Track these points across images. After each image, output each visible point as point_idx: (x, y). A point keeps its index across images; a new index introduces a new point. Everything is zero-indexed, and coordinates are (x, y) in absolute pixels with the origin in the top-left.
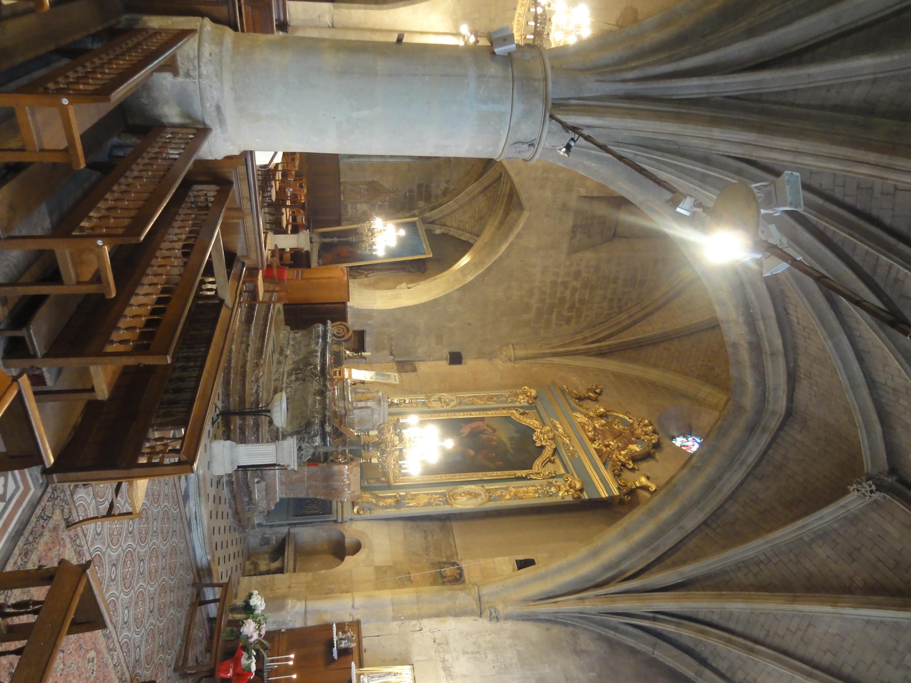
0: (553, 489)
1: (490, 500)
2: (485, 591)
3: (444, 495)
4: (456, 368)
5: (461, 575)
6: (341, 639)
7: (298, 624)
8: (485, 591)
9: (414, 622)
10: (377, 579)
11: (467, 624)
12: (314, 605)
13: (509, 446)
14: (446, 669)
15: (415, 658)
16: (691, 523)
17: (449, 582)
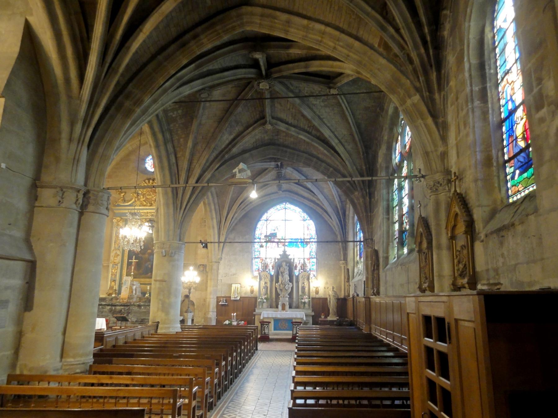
2: (214, 260)
5: (203, 265)
7: (215, 314)
8: (214, 260)
11: (221, 266)
12: (211, 309)
14: (234, 275)
15: (229, 282)
16: (216, 201)
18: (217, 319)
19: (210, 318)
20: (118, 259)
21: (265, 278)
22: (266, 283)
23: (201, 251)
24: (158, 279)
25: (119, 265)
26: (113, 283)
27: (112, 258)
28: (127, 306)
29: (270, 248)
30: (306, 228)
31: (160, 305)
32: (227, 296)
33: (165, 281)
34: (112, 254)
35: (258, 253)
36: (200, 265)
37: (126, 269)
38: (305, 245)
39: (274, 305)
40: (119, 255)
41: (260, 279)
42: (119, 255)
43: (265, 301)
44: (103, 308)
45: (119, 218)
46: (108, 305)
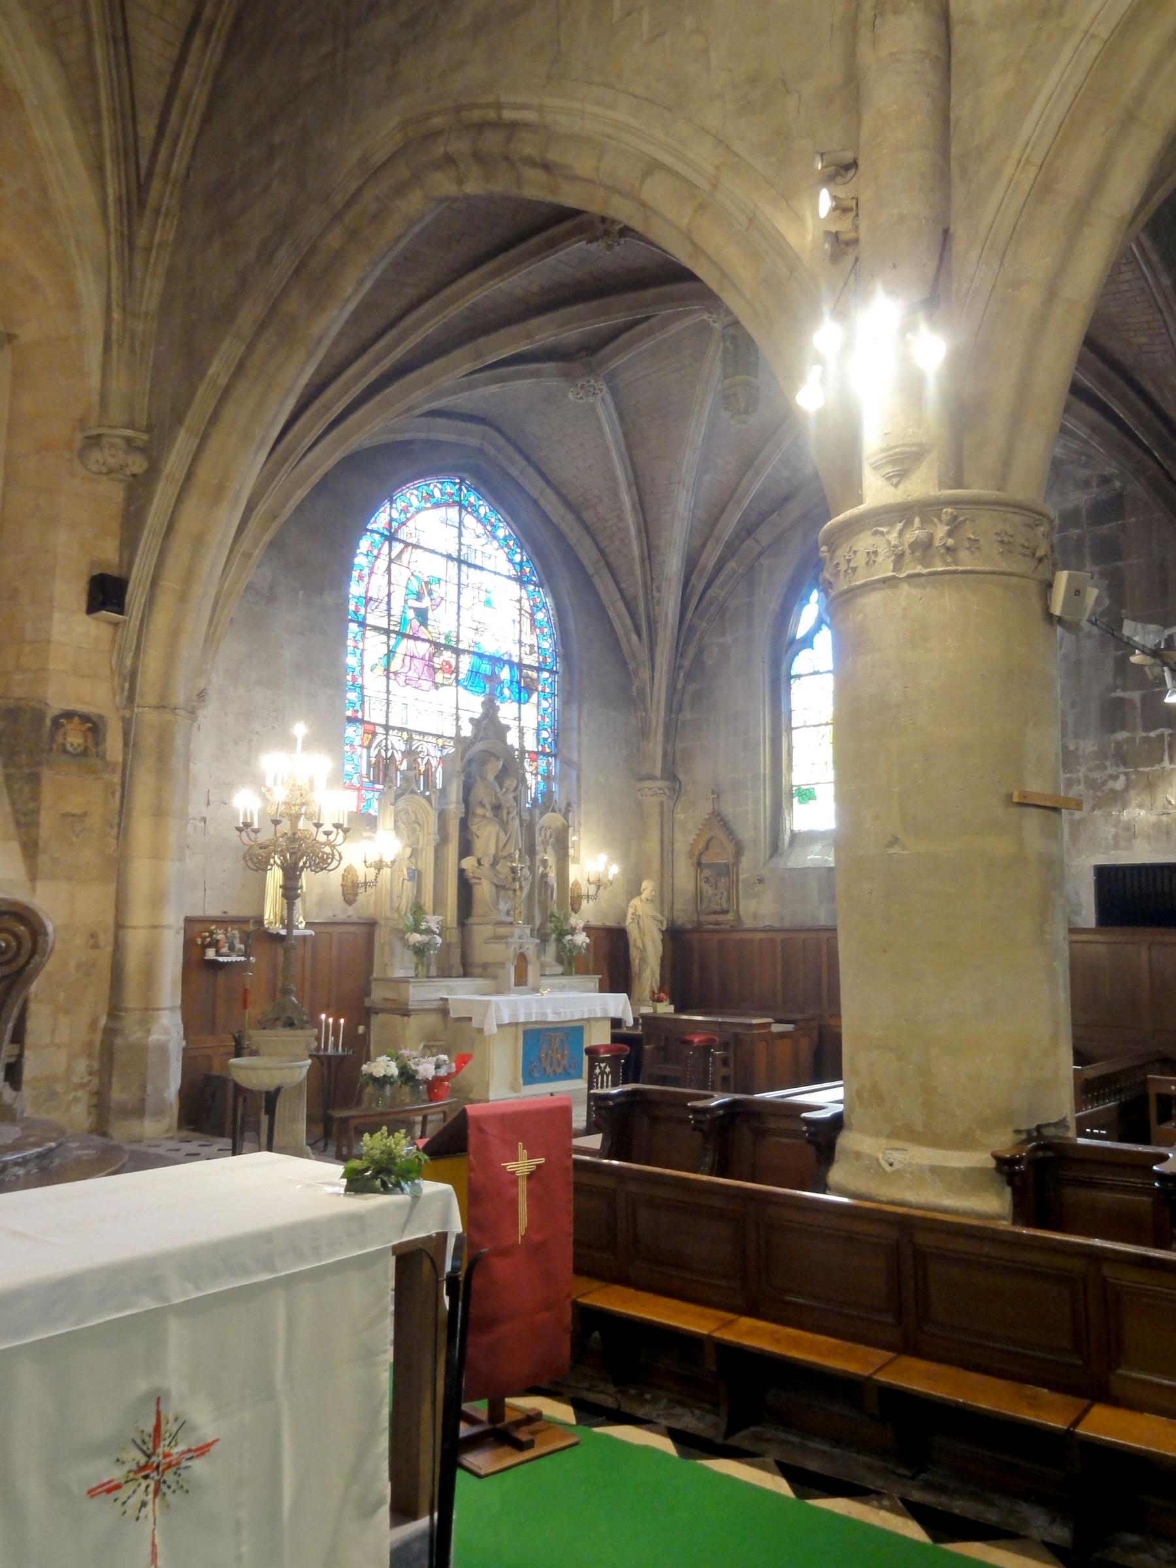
5: (85, 718)
6: (232, 948)
9: (190, 828)
10: (69, 879)
17: (97, 744)
18: (184, 1050)
19: (163, 1049)
23: (74, 630)
29: (402, 678)
30: (526, 623)
32: (233, 912)
36: (69, 715)
38: (524, 695)
39: (456, 959)
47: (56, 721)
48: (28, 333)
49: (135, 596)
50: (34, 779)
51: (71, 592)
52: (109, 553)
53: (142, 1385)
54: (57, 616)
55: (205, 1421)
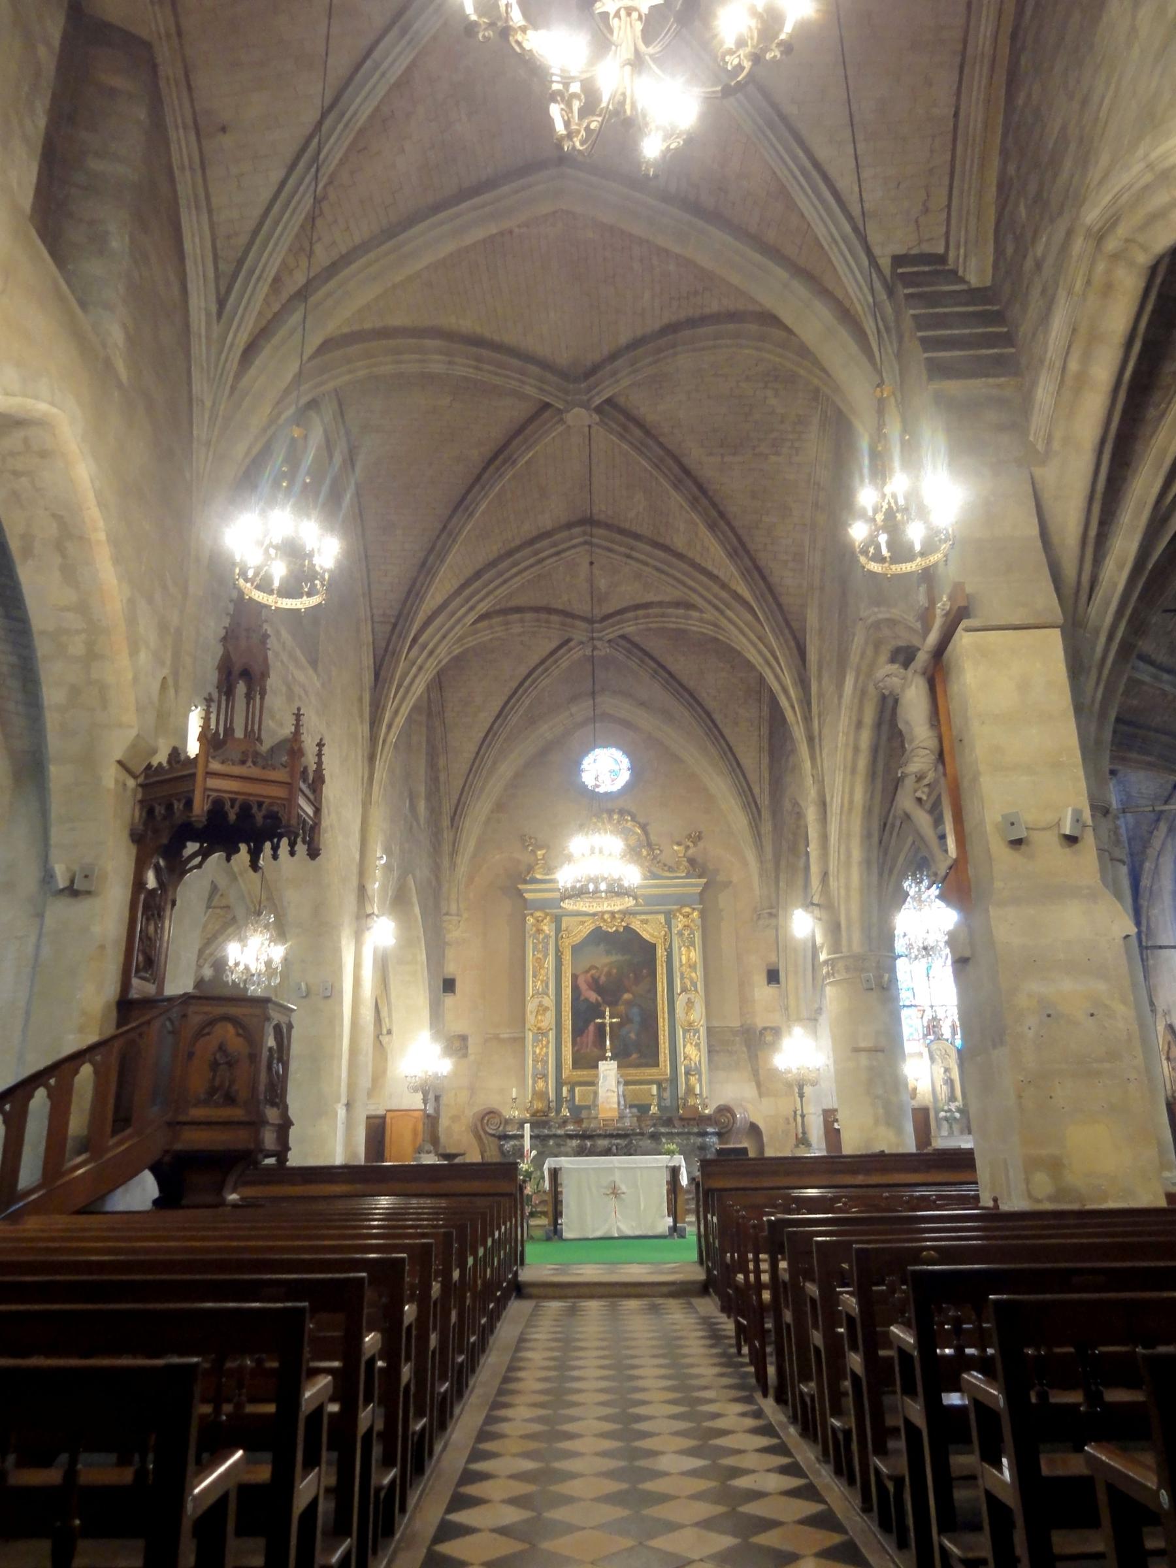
0: (686, 933)
1: (696, 990)
3: (685, 1031)
4: (458, 985)
5: (772, 1029)
13: (614, 958)
20: (548, 1020)
21: (943, 1059)
22: (947, 1070)
23: (763, 992)
24: (863, 1045)
25: (552, 1035)
26: (541, 1084)
27: (531, 1019)
28: (625, 1136)
31: (881, 1111)
33: (882, 1051)
34: (531, 1006)
35: (910, 994)
36: (765, 1029)
37: (570, 1045)
40: (547, 1009)
41: (932, 1059)
42: (547, 1009)
43: (957, 1115)
44: (559, 1145)
45: (538, 914)
46: (571, 1137)
47: (761, 1033)
48: (735, 879)
49: (782, 975)
50: (756, 1056)
51: (760, 978)
52: (773, 958)
53: (611, 1178)
54: (756, 990)
55: (624, 1188)
